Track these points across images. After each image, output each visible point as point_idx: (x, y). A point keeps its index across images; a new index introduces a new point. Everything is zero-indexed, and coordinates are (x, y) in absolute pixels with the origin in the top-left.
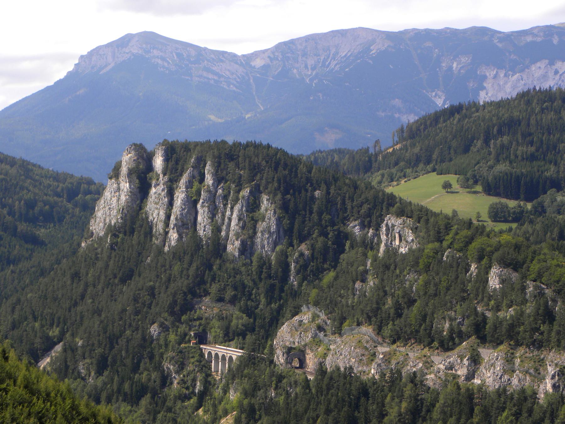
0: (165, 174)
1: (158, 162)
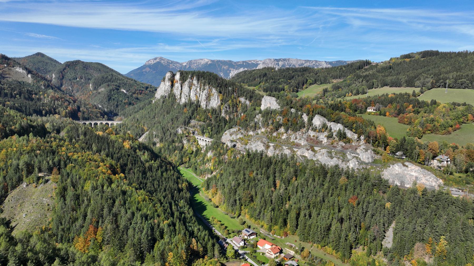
0: (180, 80)
1: (178, 77)
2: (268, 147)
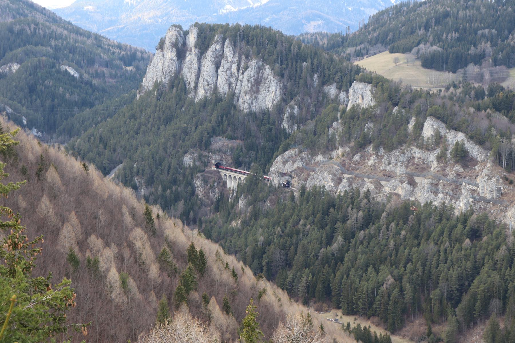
0: (196, 47)
1: (192, 39)
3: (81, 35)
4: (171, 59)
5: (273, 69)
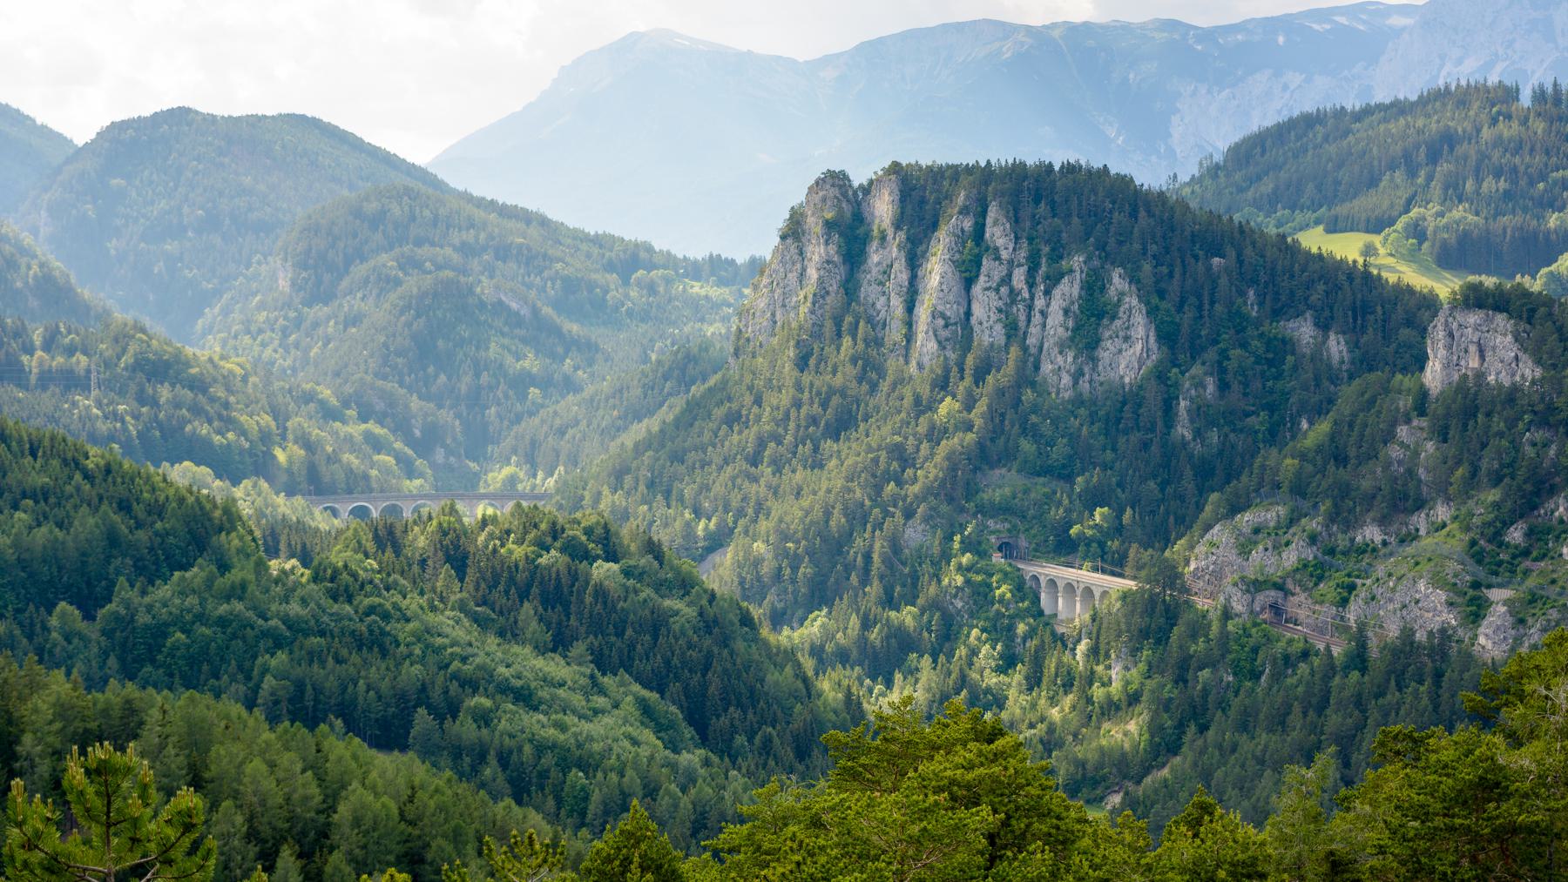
0: (897, 227)
1: (883, 209)
2: (1476, 611)
3: (510, 217)
4: (828, 262)
5: (1133, 279)
